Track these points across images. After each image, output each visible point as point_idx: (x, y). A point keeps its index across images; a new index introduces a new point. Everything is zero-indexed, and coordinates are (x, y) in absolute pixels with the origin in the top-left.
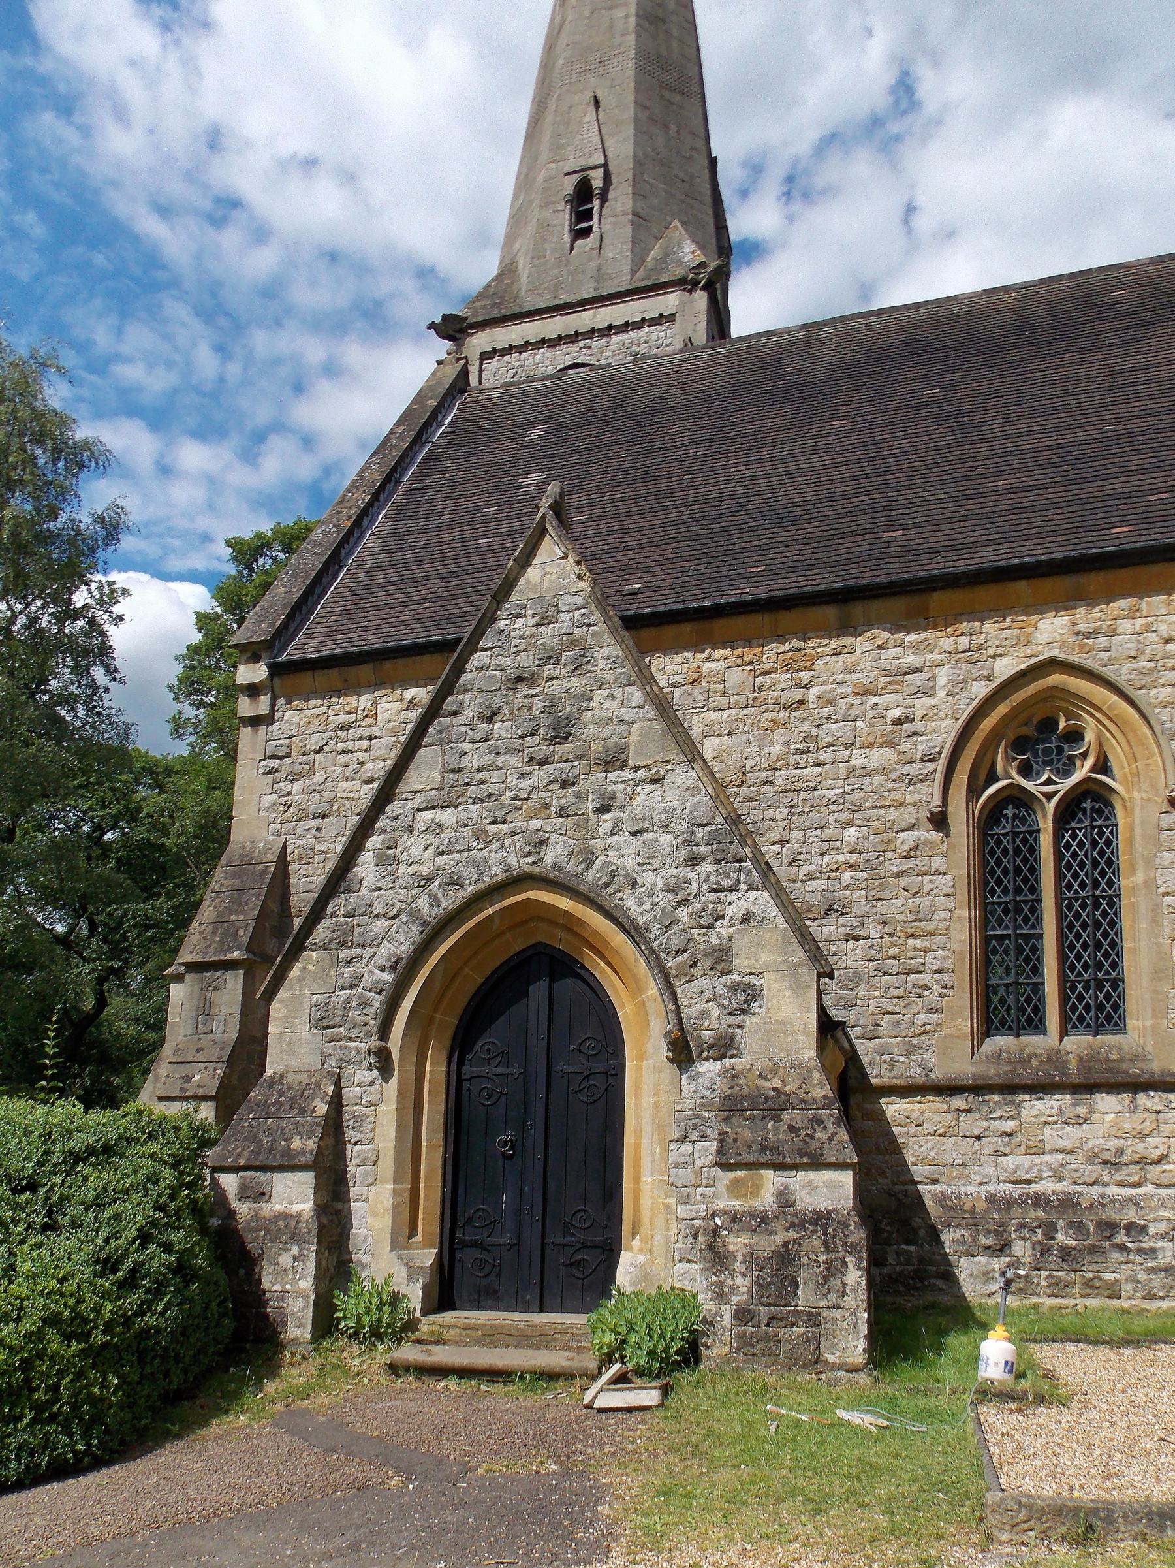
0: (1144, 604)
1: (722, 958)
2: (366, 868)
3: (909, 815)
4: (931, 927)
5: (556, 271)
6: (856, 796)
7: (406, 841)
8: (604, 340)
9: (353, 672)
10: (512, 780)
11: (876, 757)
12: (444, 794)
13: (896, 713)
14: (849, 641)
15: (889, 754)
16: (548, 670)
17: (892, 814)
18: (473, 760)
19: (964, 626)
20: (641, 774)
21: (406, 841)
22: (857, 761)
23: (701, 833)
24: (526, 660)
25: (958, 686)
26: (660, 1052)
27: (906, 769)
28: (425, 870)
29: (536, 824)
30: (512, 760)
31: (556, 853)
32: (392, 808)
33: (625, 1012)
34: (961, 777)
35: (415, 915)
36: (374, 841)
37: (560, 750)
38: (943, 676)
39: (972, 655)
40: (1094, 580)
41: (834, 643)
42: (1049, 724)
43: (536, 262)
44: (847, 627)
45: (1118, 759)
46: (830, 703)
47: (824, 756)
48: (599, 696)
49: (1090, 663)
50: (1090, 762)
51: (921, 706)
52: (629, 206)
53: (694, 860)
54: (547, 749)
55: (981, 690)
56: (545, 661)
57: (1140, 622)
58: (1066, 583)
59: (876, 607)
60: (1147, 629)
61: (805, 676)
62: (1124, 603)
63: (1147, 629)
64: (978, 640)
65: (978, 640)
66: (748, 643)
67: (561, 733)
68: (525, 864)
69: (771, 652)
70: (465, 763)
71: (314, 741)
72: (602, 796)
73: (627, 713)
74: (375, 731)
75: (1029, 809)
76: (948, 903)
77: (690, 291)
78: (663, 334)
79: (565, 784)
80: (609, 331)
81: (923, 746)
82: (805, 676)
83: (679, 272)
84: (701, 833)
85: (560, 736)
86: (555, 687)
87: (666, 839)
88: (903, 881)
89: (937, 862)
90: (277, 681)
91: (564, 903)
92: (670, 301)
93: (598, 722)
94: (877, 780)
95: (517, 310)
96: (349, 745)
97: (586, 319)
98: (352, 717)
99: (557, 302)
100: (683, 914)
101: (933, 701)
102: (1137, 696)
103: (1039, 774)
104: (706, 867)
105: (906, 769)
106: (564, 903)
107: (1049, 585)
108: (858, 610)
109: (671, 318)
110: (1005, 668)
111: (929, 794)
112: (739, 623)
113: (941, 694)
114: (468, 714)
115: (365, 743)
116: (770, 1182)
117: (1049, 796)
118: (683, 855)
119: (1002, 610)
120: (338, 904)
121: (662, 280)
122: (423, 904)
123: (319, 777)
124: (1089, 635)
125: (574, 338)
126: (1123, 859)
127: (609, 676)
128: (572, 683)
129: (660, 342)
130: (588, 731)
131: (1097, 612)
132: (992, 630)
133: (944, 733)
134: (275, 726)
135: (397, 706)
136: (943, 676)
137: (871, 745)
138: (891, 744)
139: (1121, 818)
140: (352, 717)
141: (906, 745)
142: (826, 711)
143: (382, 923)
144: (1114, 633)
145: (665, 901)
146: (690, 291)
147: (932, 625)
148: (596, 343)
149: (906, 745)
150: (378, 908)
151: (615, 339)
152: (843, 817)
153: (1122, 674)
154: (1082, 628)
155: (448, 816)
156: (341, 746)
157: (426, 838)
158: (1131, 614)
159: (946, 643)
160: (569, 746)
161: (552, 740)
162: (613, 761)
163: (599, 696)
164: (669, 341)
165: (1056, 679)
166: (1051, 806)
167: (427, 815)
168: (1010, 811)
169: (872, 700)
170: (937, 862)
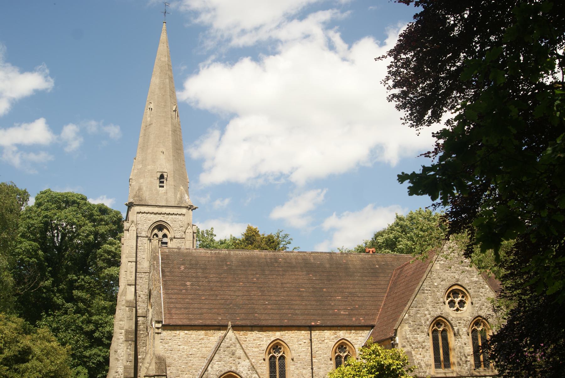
0: (289, 332)
2: (209, 368)
3: (261, 358)
4: (264, 374)
5: (156, 196)
6: (253, 355)
7: (214, 366)
8: (168, 216)
9: (176, 327)
10: (228, 359)
11: (256, 350)
12: (219, 360)
13: (259, 344)
14: (252, 332)
15: (258, 349)
16: (231, 346)
17: (258, 358)
18: (222, 356)
19: (267, 332)
20: (243, 360)
21: (214, 366)
22: (254, 350)
23: (250, 367)
24: (229, 345)
25: (266, 341)
27: (260, 352)
28: (217, 369)
29: (231, 365)
30: (227, 357)
31: (233, 369)
32: (212, 361)
34: (267, 353)
35: (216, 375)
36: (210, 365)
37: (233, 356)
39: (268, 336)
40: (283, 328)
41: (250, 332)
42: (277, 346)
43: (150, 192)
44: (252, 330)
45: (285, 352)
46: (250, 341)
47: (249, 349)
48: (238, 350)
49: (283, 340)
50: (282, 352)
51: (262, 342)
52: (173, 184)
53: (249, 370)
54: (232, 356)
55: (270, 342)
56: (231, 345)
57: (288, 334)
58: (280, 328)
59: (256, 328)
60: (289, 335)
61: (246, 337)
62: (286, 331)
63: (289, 335)
64: (269, 334)
65: (269, 334)
66: (238, 331)
67: (233, 354)
68: (229, 370)
69: (242, 333)
70: (222, 356)
71: (169, 338)
72: (239, 362)
73: (241, 353)
74: (180, 337)
75: (275, 358)
76: (266, 371)
77: (189, 210)
78: (182, 218)
79: (234, 360)
80: (169, 214)
81: (263, 348)
82: (246, 337)
83: (187, 205)
84: (250, 367)
85: (233, 354)
86: (232, 348)
87: (246, 368)
88: (260, 367)
89: (264, 365)
90: (162, 327)
91: (235, 374)
92: (184, 211)
93: (238, 353)
94: (257, 353)
95: (147, 204)
96: (176, 339)
97: (164, 210)
98: (176, 335)
99: (157, 205)
100: (248, 376)
101: (263, 342)
102: (288, 344)
103: (276, 353)
104: (250, 371)
105: (260, 352)
106: (235, 374)
107: (277, 328)
108: (254, 328)
109: (184, 215)
110: (273, 339)
111: (263, 356)
112: (237, 328)
113: (264, 341)
114: (222, 351)
115: (178, 339)
117: (277, 357)
118: (248, 370)
119: (272, 331)
120: (206, 373)
121: (182, 206)
122: (217, 374)
123: (170, 344)
124: (282, 335)
125: (160, 214)
126: (286, 366)
127: (239, 348)
128: (234, 348)
129: (181, 220)
130: (236, 354)
132: (271, 333)
133: (265, 347)
134: (162, 334)
135: (184, 334)
136: (265, 339)
137: (255, 348)
138: (258, 348)
139: (286, 360)
140: (176, 335)
141: (260, 348)
142: (249, 342)
143: (212, 375)
144: (285, 335)
145: (246, 375)
146: (189, 210)
147: (263, 331)
148: (166, 216)
149: (260, 348)
150: (212, 374)
151: (170, 216)
152: (252, 358)
153: (286, 341)
154: (281, 334)
155: (220, 363)
156: (174, 339)
157: (217, 365)
158: (287, 333)
159: (265, 334)
160: (234, 356)
161: (232, 355)
162: (239, 358)
163: (238, 350)
164: (183, 220)
165: (278, 341)
166: (278, 358)
167: (217, 363)
168: (272, 358)
169: (256, 341)
170: (264, 365)
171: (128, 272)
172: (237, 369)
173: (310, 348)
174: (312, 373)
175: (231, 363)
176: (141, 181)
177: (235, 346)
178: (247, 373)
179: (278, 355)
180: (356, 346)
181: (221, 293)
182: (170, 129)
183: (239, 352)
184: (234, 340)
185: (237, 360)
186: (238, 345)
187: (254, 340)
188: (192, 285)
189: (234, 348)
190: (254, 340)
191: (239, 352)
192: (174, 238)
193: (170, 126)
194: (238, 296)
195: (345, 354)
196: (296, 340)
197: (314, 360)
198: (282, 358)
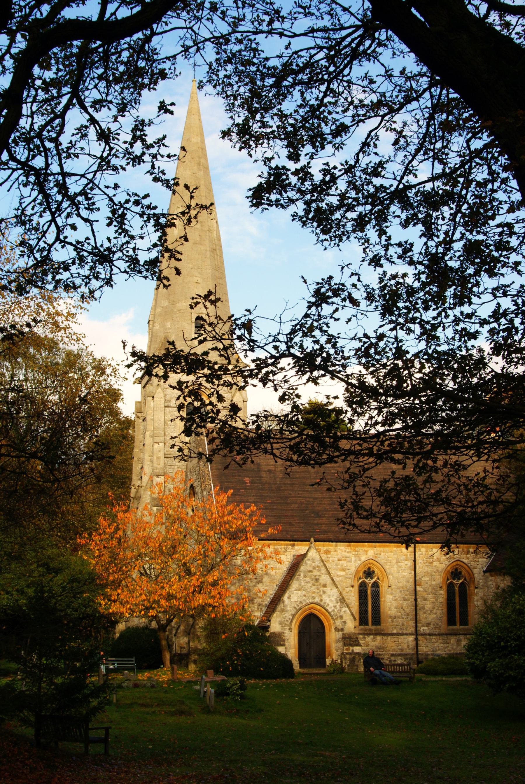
1: (341, 617)
3: (349, 585)
11: (342, 573)
18: (303, 584)
26: (333, 630)
31: (317, 600)
33: (326, 624)
38: (353, 559)
55: (359, 562)
67: (317, 580)
110: (363, 558)
116: (351, 648)
131: (379, 549)
133: (353, 569)
153: (382, 562)
155: (299, 592)
162: (325, 586)
171: (155, 457)
172: (321, 600)
173: (413, 572)
174: (416, 606)
175: (314, 593)
176: (168, 325)
177: (319, 570)
178: (335, 607)
179: (370, 582)
180: (475, 571)
181: (293, 494)
182: (208, 249)
183: (325, 579)
184: (318, 563)
185: (322, 589)
186: (323, 569)
187: (339, 560)
188: (251, 482)
189: (318, 573)
190: (339, 560)
191: (325, 579)
192: (318, 484)
193: (207, 243)
194: (316, 499)
195: (460, 581)
196: (395, 561)
197: (419, 588)
198: (376, 585)
